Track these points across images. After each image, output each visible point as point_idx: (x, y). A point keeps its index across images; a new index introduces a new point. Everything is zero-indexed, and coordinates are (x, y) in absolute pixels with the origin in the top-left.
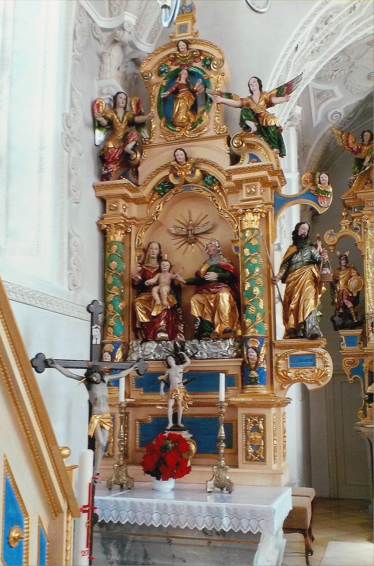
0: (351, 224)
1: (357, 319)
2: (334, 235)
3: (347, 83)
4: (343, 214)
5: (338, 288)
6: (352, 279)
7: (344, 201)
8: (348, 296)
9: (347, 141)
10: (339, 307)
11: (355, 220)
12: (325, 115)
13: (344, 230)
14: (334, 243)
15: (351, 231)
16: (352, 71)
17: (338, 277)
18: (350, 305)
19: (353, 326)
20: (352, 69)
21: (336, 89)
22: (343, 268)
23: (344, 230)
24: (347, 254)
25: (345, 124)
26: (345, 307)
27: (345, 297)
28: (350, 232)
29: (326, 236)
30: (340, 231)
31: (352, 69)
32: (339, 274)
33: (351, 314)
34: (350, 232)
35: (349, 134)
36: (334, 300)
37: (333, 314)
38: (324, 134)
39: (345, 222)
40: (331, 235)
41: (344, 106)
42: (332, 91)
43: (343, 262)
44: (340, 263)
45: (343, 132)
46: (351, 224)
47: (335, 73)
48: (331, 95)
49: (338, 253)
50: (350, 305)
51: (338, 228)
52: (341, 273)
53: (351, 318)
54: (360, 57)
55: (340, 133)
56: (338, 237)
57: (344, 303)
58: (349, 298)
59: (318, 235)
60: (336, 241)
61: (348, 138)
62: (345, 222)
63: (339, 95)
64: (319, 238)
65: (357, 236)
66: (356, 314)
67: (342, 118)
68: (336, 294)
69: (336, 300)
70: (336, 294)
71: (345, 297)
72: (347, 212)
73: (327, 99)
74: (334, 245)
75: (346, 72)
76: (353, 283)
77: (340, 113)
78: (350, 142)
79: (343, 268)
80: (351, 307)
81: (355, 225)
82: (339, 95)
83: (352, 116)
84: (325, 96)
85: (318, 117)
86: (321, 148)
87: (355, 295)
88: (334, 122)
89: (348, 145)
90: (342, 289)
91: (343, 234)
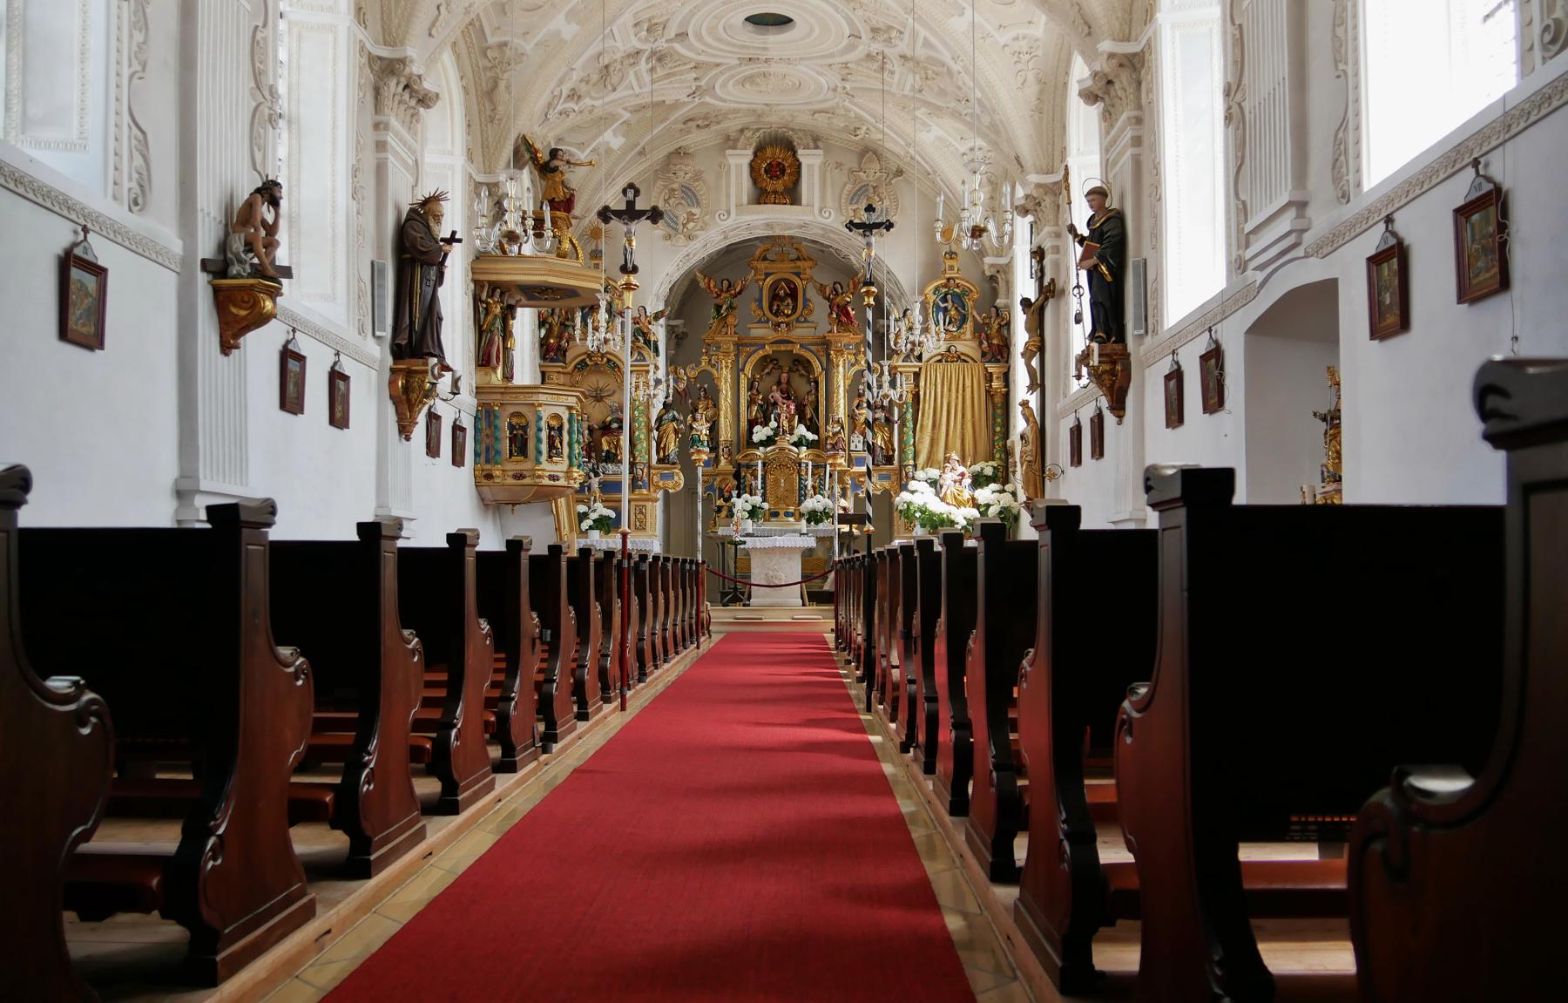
51: (698, 364)
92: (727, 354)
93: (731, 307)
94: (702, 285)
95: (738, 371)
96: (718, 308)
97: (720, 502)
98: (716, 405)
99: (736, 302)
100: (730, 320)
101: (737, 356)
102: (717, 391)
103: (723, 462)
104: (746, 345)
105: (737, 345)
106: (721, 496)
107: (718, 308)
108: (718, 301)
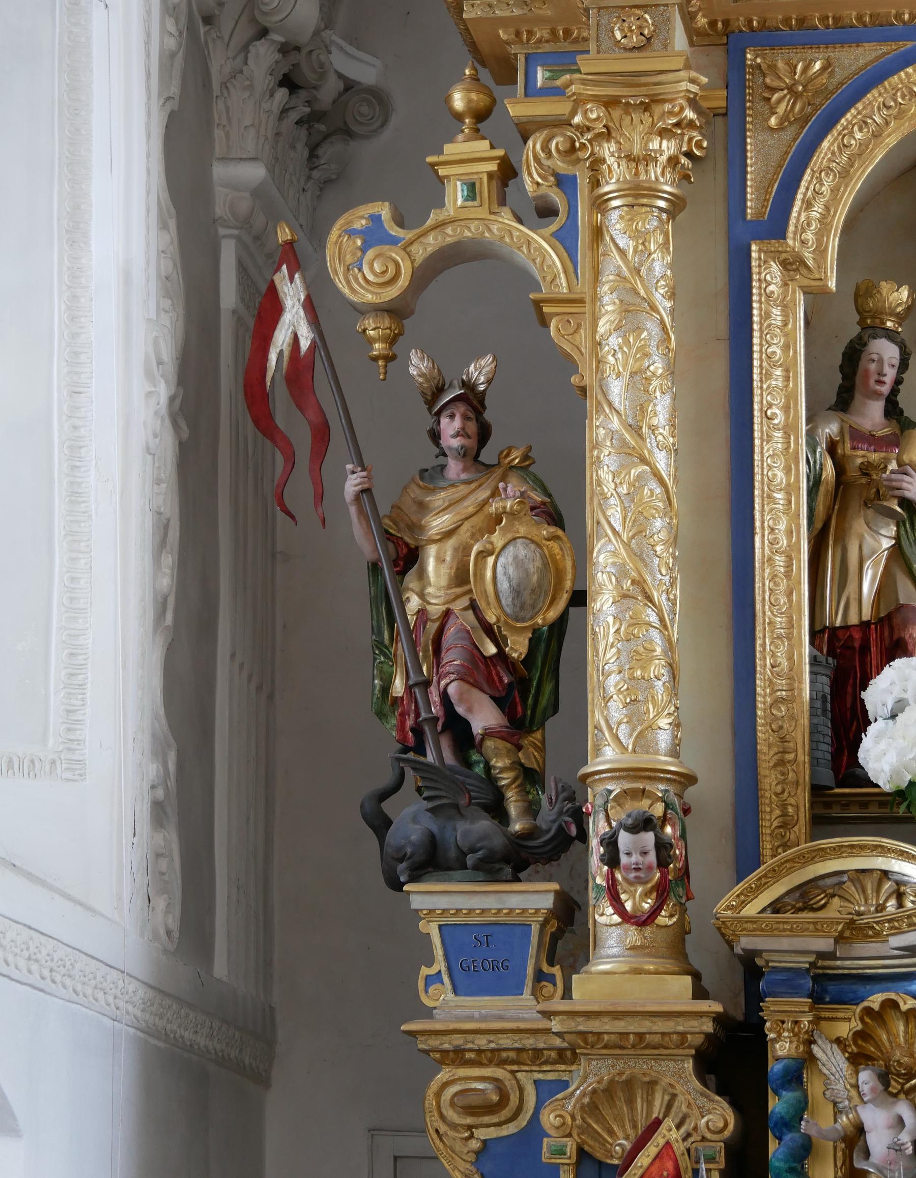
0: (507, 172)
1: (532, 809)
2: (394, 241)
4: (458, 101)
5: (414, 603)
6: (498, 539)
8: (475, 651)
10: (418, 731)
11: (535, 144)
13: (460, 210)
14: (392, 292)
15: (506, 218)
17: (416, 528)
18: (483, 716)
19: (512, 861)
22: (454, 468)
23: (460, 210)
24: (479, 371)
26: (456, 727)
27: (453, 658)
28: (503, 228)
29: (339, 245)
30: (434, 217)
32: (423, 507)
33: (490, 779)
37: (386, 778)
39: (467, 157)
40: (374, 236)
43: (450, 426)
44: (435, 436)
46: (507, 172)
49: (418, 365)
50: (483, 716)
51: (418, 196)
52: (439, 499)
53: (497, 809)
56: (420, 252)
57: (445, 697)
60: (403, 281)
62: (467, 157)
64: (291, 256)
65: (539, 249)
66: (531, 778)
69: (398, 687)
70: (402, 649)
71: (453, 658)
76: (505, 567)
79: (454, 468)
80: (488, 733)
81: (532, 182)
87: (518, 647)
90: (435, 610)
91: (451, 235)
92: (635, 97)
95: (737, 236)
98: (559, 511)
101: (726, 121)
102: (569, 401)
103: (613, 939)
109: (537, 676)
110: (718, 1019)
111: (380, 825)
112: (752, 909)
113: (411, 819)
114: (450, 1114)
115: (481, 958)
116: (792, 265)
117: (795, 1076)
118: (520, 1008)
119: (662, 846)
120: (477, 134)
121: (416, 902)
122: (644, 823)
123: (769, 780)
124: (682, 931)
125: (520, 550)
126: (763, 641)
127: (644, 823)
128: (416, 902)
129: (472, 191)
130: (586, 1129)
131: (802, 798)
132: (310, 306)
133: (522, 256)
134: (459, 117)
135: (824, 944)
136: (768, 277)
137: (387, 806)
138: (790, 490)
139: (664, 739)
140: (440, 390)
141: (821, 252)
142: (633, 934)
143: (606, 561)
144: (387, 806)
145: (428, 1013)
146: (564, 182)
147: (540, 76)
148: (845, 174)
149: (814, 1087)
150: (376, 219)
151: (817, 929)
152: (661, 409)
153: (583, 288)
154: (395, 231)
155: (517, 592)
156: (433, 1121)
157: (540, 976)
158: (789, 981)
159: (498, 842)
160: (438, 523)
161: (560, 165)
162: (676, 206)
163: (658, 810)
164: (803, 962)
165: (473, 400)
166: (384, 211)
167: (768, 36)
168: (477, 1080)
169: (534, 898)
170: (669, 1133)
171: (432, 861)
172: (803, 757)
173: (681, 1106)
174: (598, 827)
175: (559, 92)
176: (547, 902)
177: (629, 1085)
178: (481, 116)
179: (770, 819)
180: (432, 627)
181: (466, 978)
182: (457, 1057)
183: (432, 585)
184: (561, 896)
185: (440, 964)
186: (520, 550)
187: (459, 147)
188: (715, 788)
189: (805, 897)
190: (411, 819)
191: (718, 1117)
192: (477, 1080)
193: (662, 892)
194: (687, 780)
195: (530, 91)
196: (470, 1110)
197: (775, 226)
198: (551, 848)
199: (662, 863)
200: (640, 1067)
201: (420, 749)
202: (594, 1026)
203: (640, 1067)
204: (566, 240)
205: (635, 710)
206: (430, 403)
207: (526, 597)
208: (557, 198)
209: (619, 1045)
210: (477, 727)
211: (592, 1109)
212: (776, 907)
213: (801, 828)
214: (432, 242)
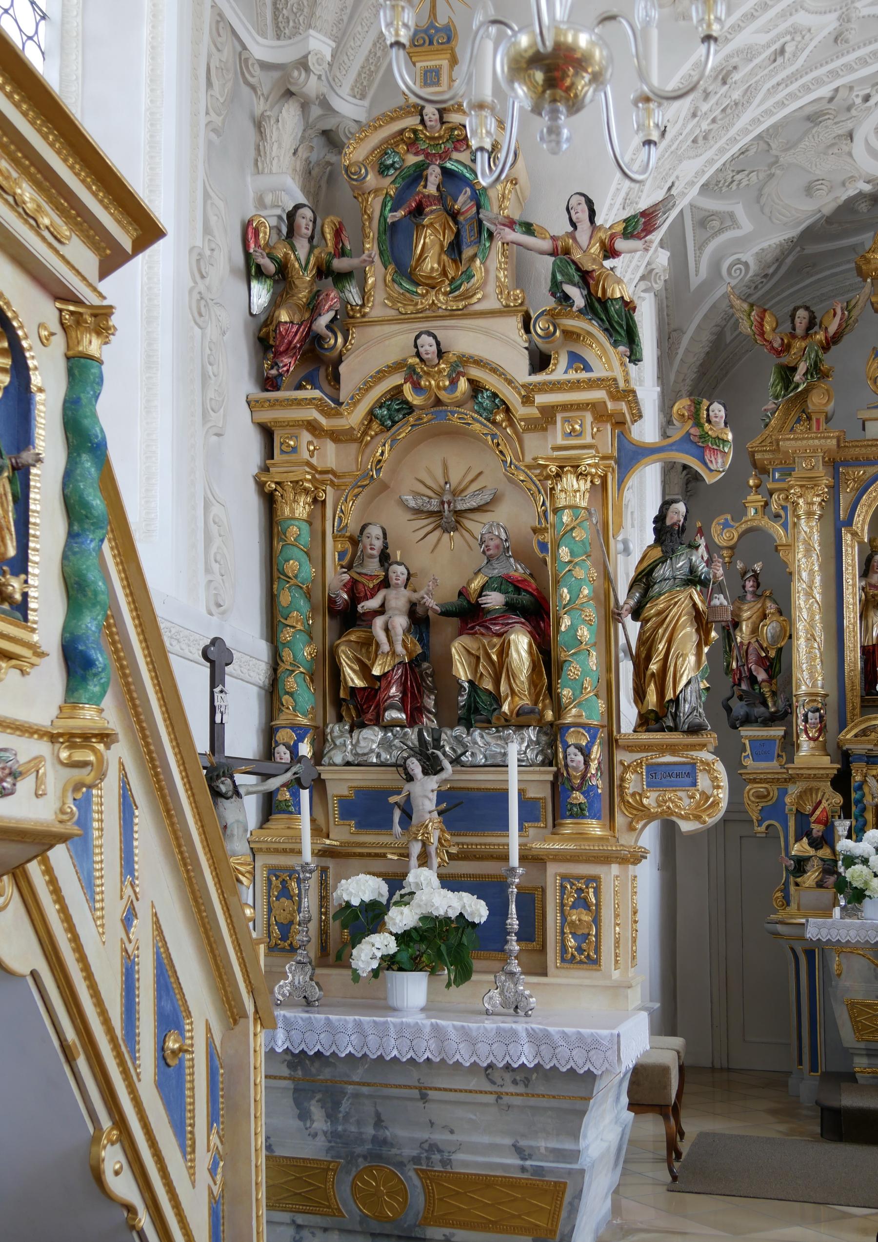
1: (775, 704)
3: (763, 200)
4: (751, 482)
5: (739, 640)
7: (752, 454)
8: (759, 655)
9: (762, 325)
10: (740, 680)
12: (715, 266)
14: (732, 543)
15: (766, 518)
16: (771, 176)
17: (739, 616)
18: (761, 676)
19: (771, 720)
20: (773, 171)
21: (740, 211)
22: (749, 597)
24: (758, 567)
25: (756, 288)
26: (753, 680)
27: (752, 658)
28: (766, 523)
30: (744, 519)
31: (773, 171)
33: (762, 695)
34: (766, 523)
35: (765, 310)
36: (729, 664)
37: (729, 694)
38: (714, 306)
39: (754, 500)
40: (726, 525)
41: (756, 249)
42: (731, 215)
43: (749, 585)
44: (744, 587)
45: (752, 306)
46: (767, 504)
47: (738, 177)
48: (728, 223)
49: (740, 565)
50: (761, 676)
51: (740, 513)
52: (745, 607)
53: (765, 704)
54: (789, 147)
55: (745, 306)
56: (740, 530)
57: (750, 670)
58: (761, 661)
59: (699, 524)
60: (735, 539)
61: (762, 319)
62: (754, 500)
63: (746, 226)
64: (700, 531)
66: (774, 694)
67: (751, 273)
68: (735, 652)
69: (734, 665)
71: (752, 658)
72: (759, 479)
73: (721, 231)
74: (731, 548)
75: (762, 175)
76: (769, 629)
77: (746, 264)
78: (767, 328)
79: (749, 597)
80: (763, 681)
81: (774, 507)
82: (746, 226)
83: (771, 271)
84: (716, 224)
85: (699, 271)
86: (706, 337)
87: (772, 654)
88: (734, 282)
89: (762, 334)
90: (746, 642)
93: (817, 371)
94: (746, 327)
95: (837, 525)
96: (787, 373)
97: (800, 848)
98: (785, 611)
99: (828, 361)
100: (817, 401)
101: (835, 490)
102: (787, 577)
103: (805, 746)
104: (857, 462)
105: (835, 465)
106: (803, 831)
107: (787, 373)
108: (786, 360)
109: (778, 664)
110: (838, 770)
111: (729, 710)
112: (848, 737)
113: (739, 708)
114: (753, 799)
115: (761, 750)
116: (854, 534)
117: (860, 788)
118: (773, 765)
119: (821, 717)
120: (757, 493)
121: (743, 733)
122: (818, 710)
123: (849, 695)
124: (825, 742)
125: (774, 624)
126: (847, 652)
127: (818, 710)
128: (743, 733)
129: (756, 513)
130: (798, 803)
131: (858, 701)
132: (707, 547)
133: (771, 531)
134: (751, 487)
135: (870, 747)
136: (847, 538)
137: (730, 703)
138: (854, 604)
139: (820, 683)
140: (745, 573)
141: (863, 530)
142: (812, 744)
143: (801, 627)
144: (730, 703)
145: (745, 767)
146: (784, 508)
147: (777, 475)
148: (870, 506)
149: (866, 789)
150: (726, 520)
151: (869, 742)
152: (818, 579)
153: (790, 541)
154: (732, 523)
155: (772, 637)
156: (746, 800)
157: (779, 756)
158: (860, 758)
159: (767, 715)
160: (746, 615)
161: (783, 503)
162: (821, 516)
163: (820, 706)
164: (863, 752)
165: (756, 576)
166: (729, 517)
167: (846, 463)
168: (761, 788)
169: (778, 732)
170: (824, 804)
171: (747, 720)
172: (858, 688)
173: (826, 796)
174: (801, 712)
175: (784, 480)
176: (782, 733)
177: (811, 790)
178: (758, 486)
179: (849, 707)
180: (745, 647)
181: (758, 756)
182: (754, 781)
183: (743, 635)
184: (786, 732)
185: (748, 752)
186: (774, 624)
187: (752, 497)
188: (833, 700)
189: (864, 733)
190: (739, 708)
191: (838, 799)
192: (761, 788)
193: (821, 731)
194: (826, 696)
195: (774, 480)
196: (758, 797)
197: (849, 522)
198: (783, 716)
199: (821, 722)
200: (814, 784)
201: (739, 685)
202: (801, 772)
203: (814, 784)
204: (785, 526)
205: (809, 673)
206: (743, 577)
207: (775, 639)
208: (782, 513)
209: (809, 777)
210: (760, 678)
211: (800, 796)
212: (856, 736)
213: (858, 711)
214: (744, 527)
